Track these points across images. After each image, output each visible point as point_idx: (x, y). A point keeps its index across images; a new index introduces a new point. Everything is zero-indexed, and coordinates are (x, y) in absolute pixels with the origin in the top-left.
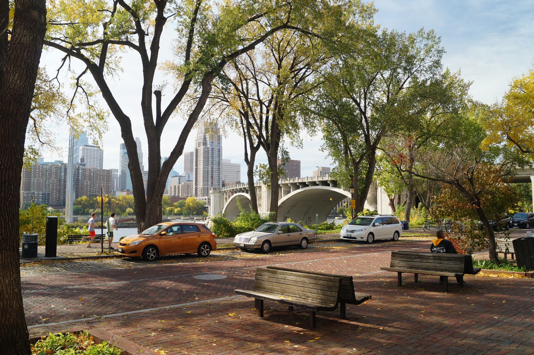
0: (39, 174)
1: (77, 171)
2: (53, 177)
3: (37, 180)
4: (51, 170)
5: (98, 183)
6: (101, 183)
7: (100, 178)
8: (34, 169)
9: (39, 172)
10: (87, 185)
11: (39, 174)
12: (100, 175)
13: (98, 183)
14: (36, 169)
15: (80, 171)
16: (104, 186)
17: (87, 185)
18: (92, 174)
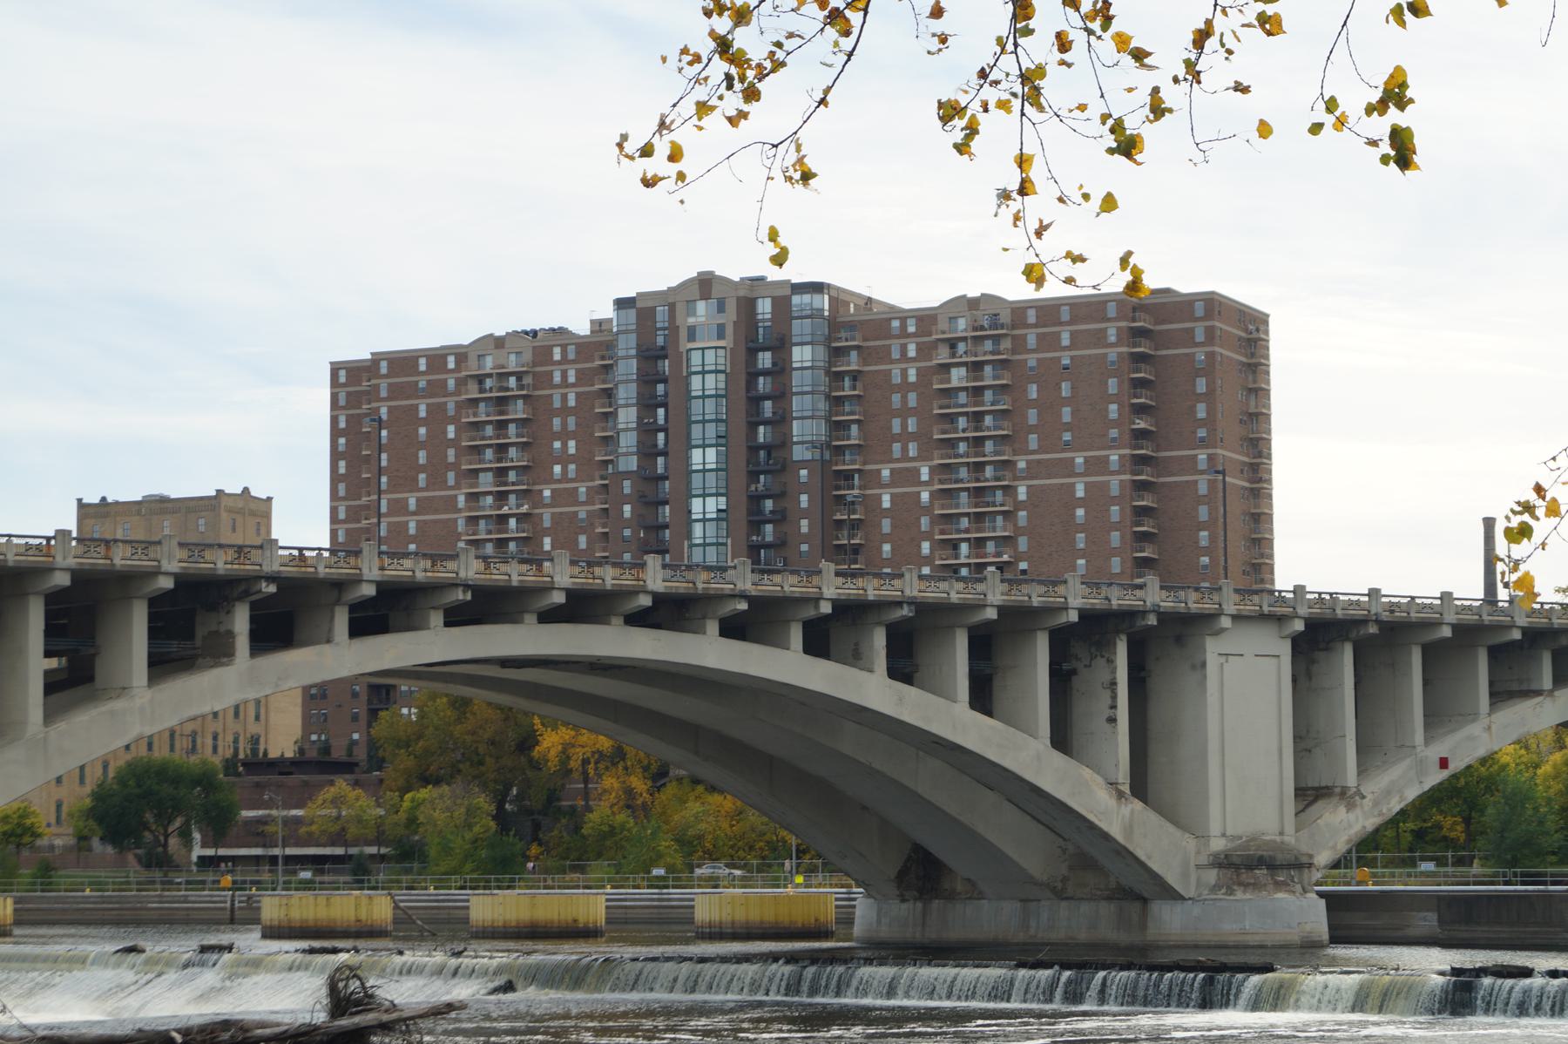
0: (437, 443)
1: (765, 359)
2: (564, 460)
3: (423, 507)
4: (544, 380)
5: (1034, 470)
6: (1067, 468)
7: (1048, 406)
8: (396, 392)
9: (437, 416)
10: (906, 507)
11: (437, 443)
12: (1049, 375)
13: (1034, 470)
14: (412, 391)
15: (801, 355)
16: (1097, 499)
17: (906, 507)
18: (958, 377)
